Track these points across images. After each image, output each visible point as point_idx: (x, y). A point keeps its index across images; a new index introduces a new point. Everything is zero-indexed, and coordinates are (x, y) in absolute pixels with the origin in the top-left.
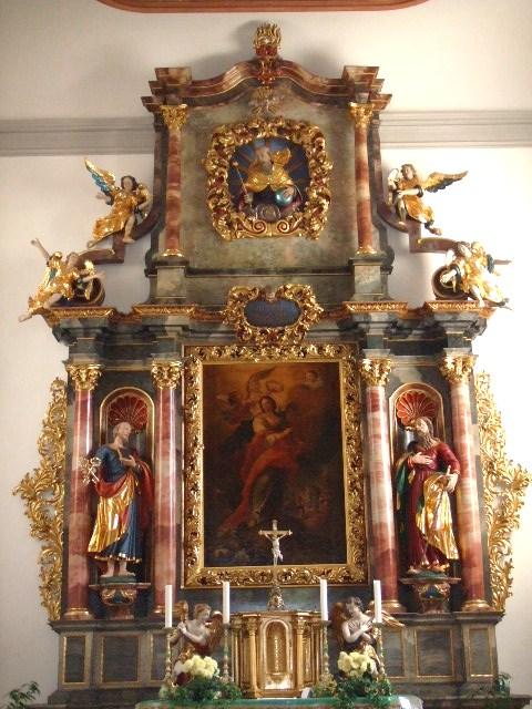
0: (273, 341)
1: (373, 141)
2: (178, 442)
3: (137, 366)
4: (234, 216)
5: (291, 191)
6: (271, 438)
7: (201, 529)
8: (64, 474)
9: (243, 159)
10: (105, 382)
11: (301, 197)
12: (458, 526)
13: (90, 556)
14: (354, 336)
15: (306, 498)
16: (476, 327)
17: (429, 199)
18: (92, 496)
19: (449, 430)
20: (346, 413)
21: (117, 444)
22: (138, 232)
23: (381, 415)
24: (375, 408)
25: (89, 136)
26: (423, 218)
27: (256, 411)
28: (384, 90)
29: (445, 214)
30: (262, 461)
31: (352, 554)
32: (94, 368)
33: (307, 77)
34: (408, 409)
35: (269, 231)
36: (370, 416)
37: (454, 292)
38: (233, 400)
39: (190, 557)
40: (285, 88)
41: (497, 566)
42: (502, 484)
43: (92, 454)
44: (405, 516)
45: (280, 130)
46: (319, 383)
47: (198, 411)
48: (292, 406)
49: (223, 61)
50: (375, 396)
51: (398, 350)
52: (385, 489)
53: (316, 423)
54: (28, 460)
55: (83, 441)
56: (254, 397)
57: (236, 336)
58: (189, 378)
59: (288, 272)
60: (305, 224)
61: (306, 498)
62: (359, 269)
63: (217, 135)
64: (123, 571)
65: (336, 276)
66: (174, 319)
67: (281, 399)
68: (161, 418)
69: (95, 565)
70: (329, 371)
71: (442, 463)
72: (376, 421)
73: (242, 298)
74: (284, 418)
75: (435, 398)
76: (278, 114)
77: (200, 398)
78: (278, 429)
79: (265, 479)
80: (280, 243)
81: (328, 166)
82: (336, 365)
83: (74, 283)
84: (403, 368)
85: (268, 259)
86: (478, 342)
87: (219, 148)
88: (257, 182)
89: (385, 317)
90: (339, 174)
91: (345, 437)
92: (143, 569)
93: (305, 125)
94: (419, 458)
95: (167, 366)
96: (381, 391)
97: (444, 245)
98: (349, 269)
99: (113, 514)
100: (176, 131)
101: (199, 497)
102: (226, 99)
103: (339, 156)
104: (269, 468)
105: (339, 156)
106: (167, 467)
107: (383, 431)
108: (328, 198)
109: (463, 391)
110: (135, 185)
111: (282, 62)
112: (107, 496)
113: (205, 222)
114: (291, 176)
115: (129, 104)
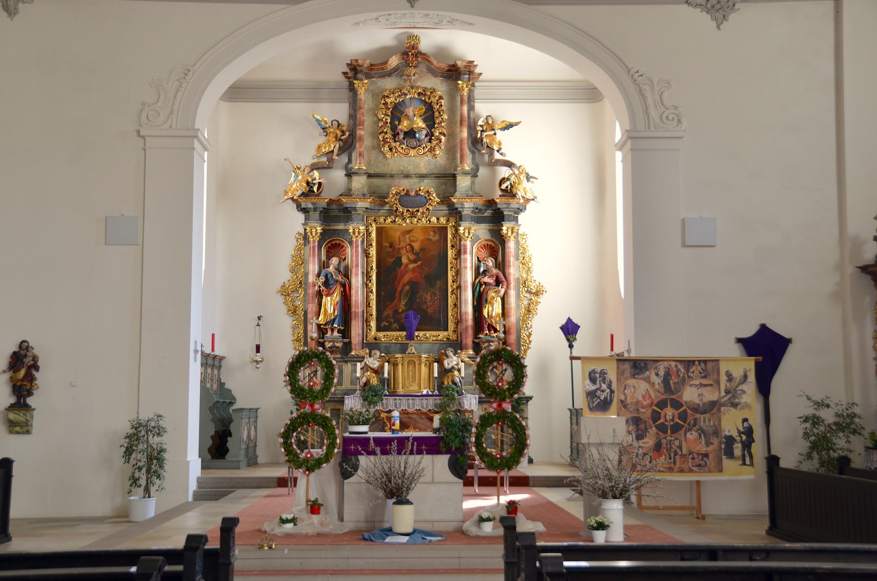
0: (413, 215)
1: (471, 99)
2: (363, 268)
3: (341, 227)
4: (393, 144)
5: (424, 132)
6: (411, 266)
7: (374, 313)
8: (302, 283)
9: (397, 113)
10: (324, 234)
11: (430, 135)
12: (504, 314)
13: (319, 326)
14: (455, 213)
15: (429, 298)
16: (519, 210)
17: (501, 135)
18: (320, 295)
19: (502, 265)
20: (451, 253)
21: (331, 269)
22: (342, 150)
23: (468, 256)
24: (465, 253)
25: (314, 92)
26: (496, 148)
27: (403, 252)
28: (477, 71)
29: (509, 145)
30: (406, 278)
31: (451, 326)
32: (319, 229)
33: (435, 62)
34: (483, 253)
35: (412, 152)
36: (462, 256)
37: (510, 193)
38: (391, 246)
39: (368, 326)
40: (423, 67)
41: (524, 334)
42: (530, 292)
43: (319, 275)
44: (478, 308)
45: (419, 94)
46: (437, 237)
47: (373, 251)
48: (422, 249)
49: (387, 51)
50: (465, 246)
51: (479, 220)
52: (468, 296)
54: (284, 276)
55: (313, 267)
56: (403, 244)
57: (393, 212)
58: (369, 234)
59: (422, 176)
60: (432, 150)
61: (429, 298)
62: (459, 178)
63: (384, 97)
64: (336, 334)
65: (448, 178)
66: (361, 204)
67: (416, 246)
68: (353, 255)
69: (322, 330)
70: (443, 230)
71: (498, 282)
72: (466, 260)
73: (397, 193)
74: (419, 256)
75: (496, 247)
76: (418, 84)
77: (374, 244)
78: (415, 261)
79: (407, 287)
80: (417, 160)
81: (445, 117)
82: (446, 228)
83: (308, 183)
84: (482, 231)
85: (411, 170)
86: (521, 217)
87: (386, 104)
88: (404, 125)
89: (472, 205)
90: (451, 122)
91: (449, 266)
92: (345, 332)
93: (433, 91)
94: (486, 279)
95: (356, 228)
96: (468, 243)
98: (454, 176)
99: (331, 303)
100: (362, 92)
101: (373, 297)
102: (390, 74)
103: (452, 111)
104: (410, 282)
105: (452, 111)
106: (357, 281)
107: (469, 265)
108: (444, 135)
109: (511, 245)
110: (339, 125)
111: (420, 53)
112: (327, 296)
113: (378, 148)
114: (425, 121)
115: (335, 74)
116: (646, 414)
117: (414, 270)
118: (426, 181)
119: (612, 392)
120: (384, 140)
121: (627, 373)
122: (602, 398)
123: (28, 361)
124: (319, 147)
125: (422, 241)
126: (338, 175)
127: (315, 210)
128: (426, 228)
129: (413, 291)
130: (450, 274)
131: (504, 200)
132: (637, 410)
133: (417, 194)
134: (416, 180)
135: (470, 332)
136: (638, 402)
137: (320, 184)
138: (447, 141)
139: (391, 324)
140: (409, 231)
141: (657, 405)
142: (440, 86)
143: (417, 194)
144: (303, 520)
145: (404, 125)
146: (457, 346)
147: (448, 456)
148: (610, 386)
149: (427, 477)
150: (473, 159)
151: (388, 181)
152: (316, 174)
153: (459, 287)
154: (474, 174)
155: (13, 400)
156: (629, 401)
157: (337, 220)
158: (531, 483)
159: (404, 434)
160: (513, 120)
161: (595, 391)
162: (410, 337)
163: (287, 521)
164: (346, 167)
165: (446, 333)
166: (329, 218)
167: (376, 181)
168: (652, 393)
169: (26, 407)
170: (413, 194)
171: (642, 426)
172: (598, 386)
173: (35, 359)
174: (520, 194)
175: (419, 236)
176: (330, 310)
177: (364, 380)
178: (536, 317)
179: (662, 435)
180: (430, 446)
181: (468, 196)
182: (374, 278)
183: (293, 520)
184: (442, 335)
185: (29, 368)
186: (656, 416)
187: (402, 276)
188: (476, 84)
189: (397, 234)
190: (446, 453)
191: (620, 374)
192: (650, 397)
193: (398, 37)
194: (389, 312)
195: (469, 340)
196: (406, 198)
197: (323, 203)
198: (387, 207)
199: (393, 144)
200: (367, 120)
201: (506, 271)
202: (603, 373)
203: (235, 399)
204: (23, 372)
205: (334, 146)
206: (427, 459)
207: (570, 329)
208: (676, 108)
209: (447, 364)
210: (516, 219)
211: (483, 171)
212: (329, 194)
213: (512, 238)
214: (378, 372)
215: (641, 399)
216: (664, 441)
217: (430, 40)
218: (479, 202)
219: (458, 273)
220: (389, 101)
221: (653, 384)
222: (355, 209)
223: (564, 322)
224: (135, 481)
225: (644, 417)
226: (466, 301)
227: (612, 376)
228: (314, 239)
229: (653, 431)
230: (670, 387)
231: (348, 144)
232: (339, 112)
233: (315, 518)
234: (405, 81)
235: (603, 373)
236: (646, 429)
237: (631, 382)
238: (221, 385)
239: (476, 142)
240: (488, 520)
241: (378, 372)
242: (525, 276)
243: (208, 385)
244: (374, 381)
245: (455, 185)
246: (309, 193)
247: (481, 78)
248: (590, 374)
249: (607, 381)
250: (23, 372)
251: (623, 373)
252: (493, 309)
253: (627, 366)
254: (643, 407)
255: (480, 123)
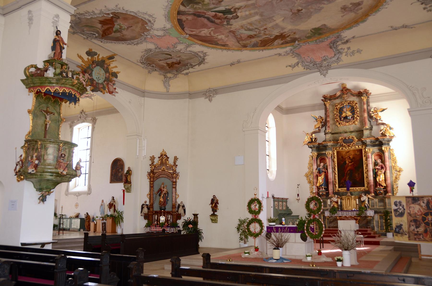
0: (349, 146)
1: (368, 102)
2: (332, 166)
3: (324, 152)
4: (340, 122)
5: (351, 116)
6: (350, 164)
7: (337, 181)
8: (312, 173)
9: (341, 111)
10: (318, 156)
11: (353, 117)
12: (385, 180)
13: (317, 187)
14: (364, 144)
15: (357, 175)
16: (389, 141)
17: (380, 114)
18: (317, 176)
19: (383, 161)
20: (364, 158)
21: (321, 167)
22: (323, 126)
23: (370, 159)
24: (369, 158)
25: (313, 108)
26: (378, 118)
27: (347, 159)
28: (370, 92)
29: (384, 117)
30: (348, 169)
31: (366, 185)
32: (316, 154)
33: (353, 92)
34: (377, 158)
35: (347, 124)
36: (368, 159)
37: (384, 135)
38: (342, 157)
39: (335, 186)
40: (349, 94)
41: (395, 186)
42: (396, 171)
43: (317, 169)
44: (375, 178)
45: (348, 103)
46: (359, 153)
47: (336, 160)
48: (353, 158)
49: (336, 90)
50: (369, 156)
51: (374, 146)
52: (371, 174)
53: (358, 160)
54: (306, 170)
55: (315, 167)
56: (346, 156)
57: (342, 146)
58: (334, 154)
59: (351, 132)
60: (354, 122)
61: (357, 175)
62: (364, 131)
63: (336, 106)
64: (323, 189)
65: (360, 132)
66: (329, 144)
67: (351, 157)
68: (329, 162)
69: (318, 188)
70: (361, 150)
71: (382, 168)
72: (369, 161)
73: (342, 139)
74: (352, 160)
75: (381, 155)
76: (348, 100)
77: (336, 157)
78: (351, 162)
79: (349, 172)
80: (349, 126)
81: (358, 110)
82: (362, 150)
83: (311, 139)
84: (376, 149)
85: (347, 130)
86: (391, 143)
87: (337, 108)
88: (344, 115)
89: (369, 140)
90: (361, 111)
91: (364, 163)
92: (327, 189)
93: (353, 102)
94: (377, 167)
95: (329, 152)
96: (370, 154)
97: (383, 124)
98: (363, 131)
99: (321, 179)
100: (328, 105)
101: (337, 176)
102: (337, 98)
103: (361, 107)
104: (349, 170)
105: (361, 107)
106: (330, 171)
107: (371, 162)
108: (358, 116)
109: (387, 154)
110: (321, 117)
111: (348, 89)
112: (320, 176)
113: (335, 124)
114: (351, 112)
115: (319, 100)
116: (419, 218)
117: (351, 165)
118: (353, 133)
119: (404, 209)
120: (337, 121)
121: (410, 202)
122: (400, 212)
123: (215, 201)
124: (315, 126)
125: (353, 155)
126: (322, 134)
127: (314, 147)
128: (354, 150)
129: (352, 172)
130: (364, 166)
131: (382, 137)
132: (416, 217)
133: (349, 139)
134: (349, 133)
135: (372, 187)
136: (416, 213)
137: (315, 138)
138: (360, 118)
139: (343, 185)
140: (348, 152)
141: (424, 215)
142: (355, 99)
143: (349, 139)
144: (252, 253)
145: (344, 115)
146: (367, 192)
147: (300, 234)
148: (403, 207)
149: (290, 241)
150: (370, 124)
151: (339, 135)
152: (314, 135)
153: (368, 171)
154: (371, 129)
155: (212, 213)
156: (412, 213)
157: (323, 150)
158: (381, 244)
159: (286, 226)
160: (384, 108)
161: (397, 209)
162: (348, 190)
163: (246, 253)
164: (325, 132)
165: (364, 188)
166: (320, 149)
167: (335, 135)
168: (422, 210)
169: (216, 215)
170: (347, 138)
171: (418, 223)
172: (398, 207)
173: (217, 201)
174: (387, 134)
175: (353, 153)
176: (321, 181)
177: (332, 205)
178: (400, 180)
179: (427, 227)
180: (293, 230)
181: (368, 137)
182: (336, 169)
183: (248, 253)
184: (362, 188)
185: (216, 203)
186: (424, 219)
187: (347, 168)
188: (370, 97)
189: (344, 153)
190: (299, 232)
191: (407, 202)
192: (421, 211)
193: (339, 85)
194: (342, 181)
195: (372, 190)
196: (345, 140)
197: (316, 144)
198: (339, 144)
199: (340, 122)
200: (331, 115)
201: (386, 163)
202: (400, 202)
203: (292, 212)
204: (214, 205)
205: (320, 125)
206: (292, 234)
207: (411, 184)
208: (429, 98)
209: (362, 199)
210: (388, 144)
211: (375, 128)
212: (319, 141)
213: (387, 152)
214: (337, 202)
215: (417, 212)
216: (428, 229)
217: (350, 85)
218: (373, 139)
219: (367, 165)
220: (337, 107)
221: (422, 206)
222: (327, 146)
223: (409, 182)
224: (241, 239)
225: (419, 219)
226: (370, 176)
227: (404, 203)
228: (315, 157)
229: (423, 225)
230: (430, 207)
231: (324, 124)
232: (322, 113)
233: (256, 252)
234: (343, 99)
235: (400, 202)
236: (420, 224)
237: (412, 205)
238: (287, 208)
239: (370, 117)
240: (309, 256)
241: (337, 202)
242: (394, 165)
243: (277, 208)
244: (336, 206)
245: (363, 134)
246: (311, 142)
247: (371, 94)
248: (395, 203)
249: (402, 205)
250: (214, 205)
251: (408, 202)
252: (381, 178)
253: (410, 199)
254: (418, 215)
255: (372, 110)
